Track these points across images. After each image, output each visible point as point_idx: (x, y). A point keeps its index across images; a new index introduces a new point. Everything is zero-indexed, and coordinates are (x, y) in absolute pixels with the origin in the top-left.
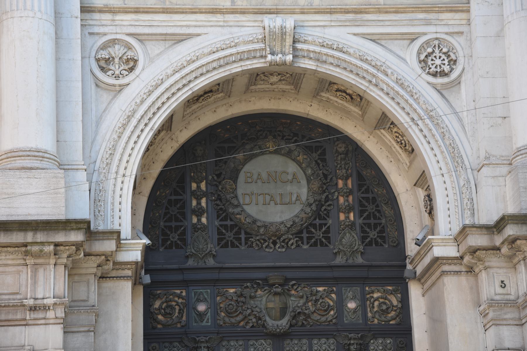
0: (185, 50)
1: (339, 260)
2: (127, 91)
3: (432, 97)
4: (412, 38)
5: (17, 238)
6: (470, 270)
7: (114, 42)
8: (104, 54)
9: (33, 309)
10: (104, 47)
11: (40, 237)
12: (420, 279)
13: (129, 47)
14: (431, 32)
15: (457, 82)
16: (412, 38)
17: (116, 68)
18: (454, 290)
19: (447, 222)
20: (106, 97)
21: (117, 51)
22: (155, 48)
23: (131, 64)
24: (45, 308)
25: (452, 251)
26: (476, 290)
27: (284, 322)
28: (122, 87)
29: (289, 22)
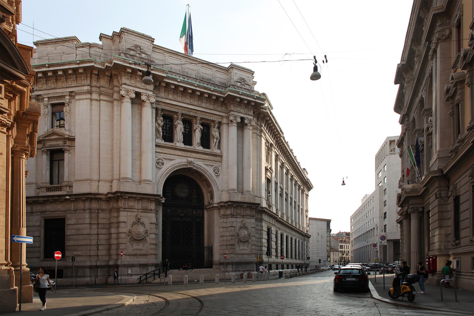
0: (173, 162)
1: (193, 204)
2: (162, 169)
3: (215, 177)
4: (212, 166)
5: (148, 197)
6: (219, 209)
7: (160, 159)
8: (158, 161)
9: (150, 210)
10: (158, 160)
11: (152, 197)
12: (207, 209)
13: (162, 160)
14: (216, 165)
15: (219, 175)
16: (212, 166)
17: (160, 164)
18: (216, 212)
19: (216, 200)
20: (158, 170)
21: (161, 161)
22: (168, 161)
23: (163, 164)
24: (152, 210)
25: (216, 205)
26: (219, 213)
27: (183, 215)
28: (161, 168)
29: (193, 160)
